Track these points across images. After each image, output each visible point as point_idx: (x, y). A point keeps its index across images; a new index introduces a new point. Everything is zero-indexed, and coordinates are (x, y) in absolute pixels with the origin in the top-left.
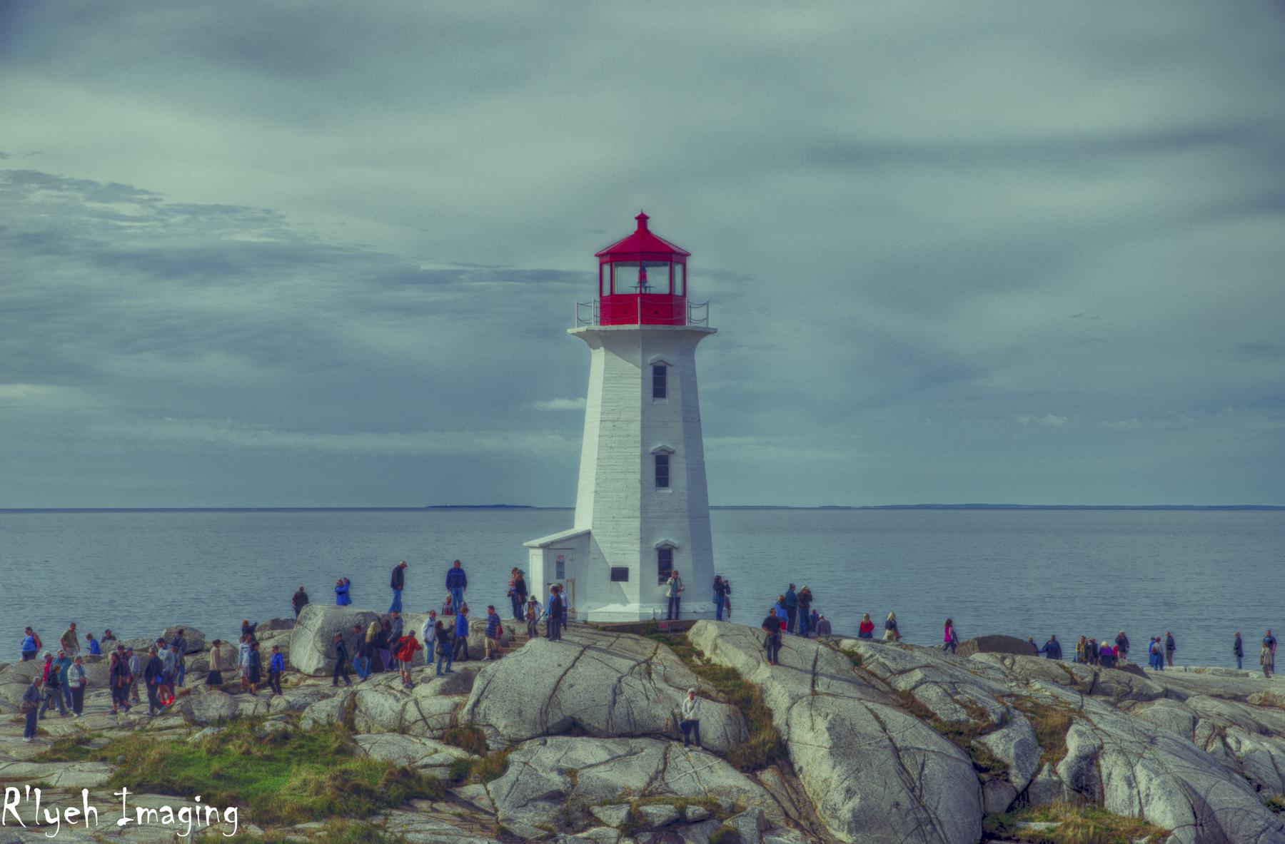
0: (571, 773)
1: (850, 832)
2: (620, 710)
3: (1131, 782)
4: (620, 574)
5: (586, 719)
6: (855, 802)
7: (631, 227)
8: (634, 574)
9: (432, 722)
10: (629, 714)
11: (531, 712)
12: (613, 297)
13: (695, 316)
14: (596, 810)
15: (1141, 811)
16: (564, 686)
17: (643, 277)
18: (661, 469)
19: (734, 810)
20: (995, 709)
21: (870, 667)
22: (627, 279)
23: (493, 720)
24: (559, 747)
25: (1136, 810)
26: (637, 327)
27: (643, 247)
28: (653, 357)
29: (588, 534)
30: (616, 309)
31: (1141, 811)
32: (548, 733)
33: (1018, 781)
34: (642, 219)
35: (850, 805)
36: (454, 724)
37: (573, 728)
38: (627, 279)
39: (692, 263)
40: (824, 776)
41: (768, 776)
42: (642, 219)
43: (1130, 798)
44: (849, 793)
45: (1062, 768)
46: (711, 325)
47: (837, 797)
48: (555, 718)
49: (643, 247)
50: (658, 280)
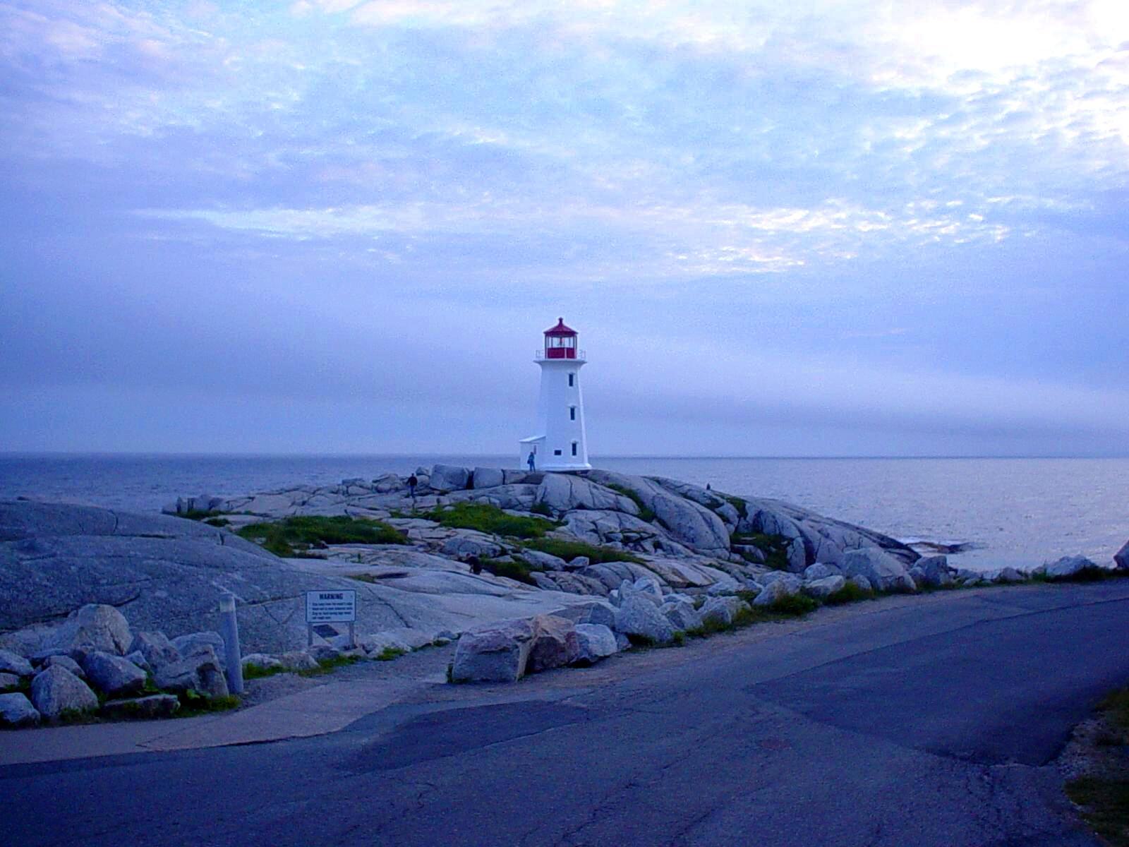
0: (594, 523)
2: (596, 502)
3: (775, 522)
4: (558, 453)
5: (585, 502)
7: (556, 323)
10: (600, 501)
11: (566, 501)
12: (553, 349)
13: (579, 357)
15: (780, 533)
16: (574, 491)
17: (561, 342)
19: (654, 535)
20: (721, 501)
22: (555, 342)
24: (583, 513)
25: (778, 532)
26: (565, 359)
27: (560, 331)
28: (569, 371)
30: (553, 353)
31: (780, 533)
33: (736, 524)
34: (561, 320)
35: (692, 532)
36: (534, 506)
37: (581, 507)
38: (555, 342)
39: (578, 336)
40: (677, 523)
41: (654, 522)
42: (561, 320)
45: (748, 519)
46: (586, 360)
48: (575, 504)
49: (560, 331)
50: (567, 343)
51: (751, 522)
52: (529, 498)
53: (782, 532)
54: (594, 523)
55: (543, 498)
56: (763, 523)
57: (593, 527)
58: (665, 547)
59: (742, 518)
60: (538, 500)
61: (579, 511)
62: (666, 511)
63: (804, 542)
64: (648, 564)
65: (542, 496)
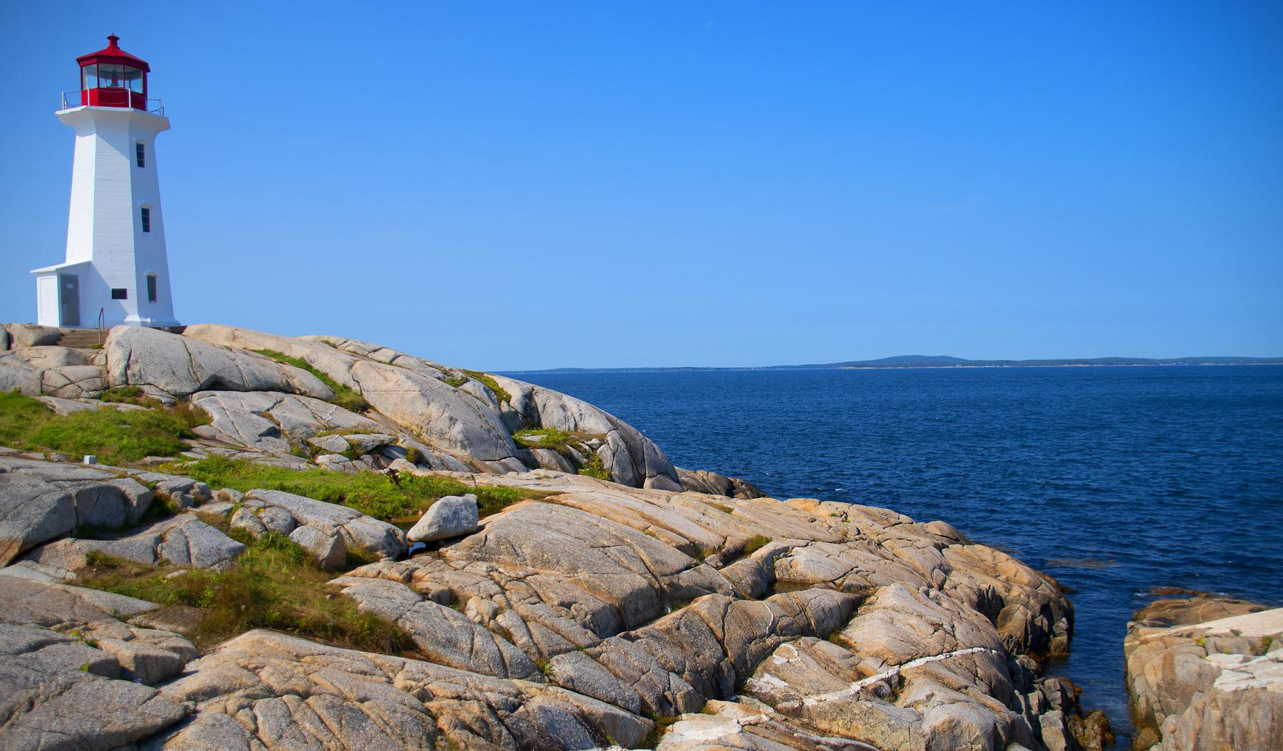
0: (265, 414)
1: (464, 447)
3: (564, 408)
5: (227, 376)
6: (459, 427)
8: (132, 293)
9: (81, 384)
11: (182, 373)
14: (314, 441)
15: (576, 425)
18: (145, 219)
21: (351, 348)
23: (151, 380)
25: (572, 426)
29: (89, 264)
31: (576, 425)
32: (200, 389)
35: (459, 427)
37: (216, 384)
43: (566, 419)
44: (453, 420)
47: (443, 424)
51: (520, 409)
52: (90, 370)
53: (581, 425)
54: (265, 414)
55: (127, 367)
56: (540, 409)
57: (266, 425)
58: (431, 461)
59: (504, 403)
60: (116, 372)
61: (217, 393)
62: (387, 391)
63: (623, 439)
64: (561, 498)
65: (123, 363)
